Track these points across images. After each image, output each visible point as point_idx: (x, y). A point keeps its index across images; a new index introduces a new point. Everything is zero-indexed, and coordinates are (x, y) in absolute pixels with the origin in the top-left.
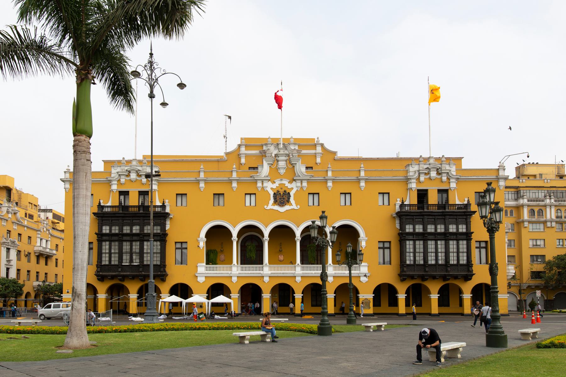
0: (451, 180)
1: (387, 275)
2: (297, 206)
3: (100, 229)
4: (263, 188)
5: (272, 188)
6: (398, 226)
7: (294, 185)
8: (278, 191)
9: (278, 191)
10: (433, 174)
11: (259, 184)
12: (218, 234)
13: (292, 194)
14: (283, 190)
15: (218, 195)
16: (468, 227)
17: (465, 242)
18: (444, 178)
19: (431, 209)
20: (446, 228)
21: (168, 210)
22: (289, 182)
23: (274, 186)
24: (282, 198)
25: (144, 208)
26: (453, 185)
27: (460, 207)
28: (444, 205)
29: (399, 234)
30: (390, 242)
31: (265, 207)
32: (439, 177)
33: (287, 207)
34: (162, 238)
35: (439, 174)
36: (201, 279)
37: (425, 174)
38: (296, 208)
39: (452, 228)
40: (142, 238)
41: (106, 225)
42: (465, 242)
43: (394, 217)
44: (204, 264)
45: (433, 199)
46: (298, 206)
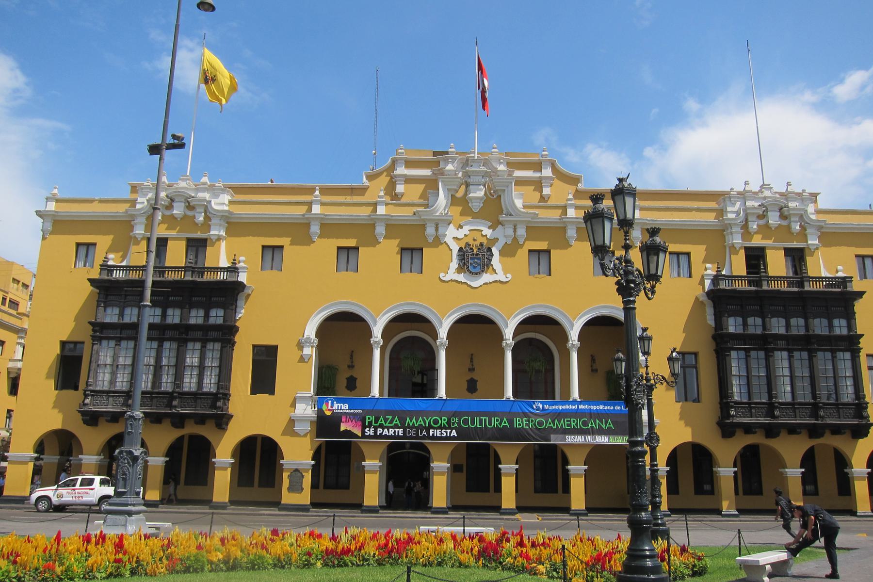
0: (808, 231)
2: (505, 274)
5: (456, 239)
6: (710, 321)
7: (499, 232)
8: (468, 245)
9: (468, 245)
11: (430, 230)
14: (478, 243)
16: (851, 326)
17: (848, 355)
19: (775, 286)
22: (489, 228)
23: (460, 234)
24: (474, 259)
29: (714, 337)
30: (696, 354)
31: (442, 275)
33: (486, 277)
35: (783, 217)
38: (504, 280)
43: (702, 302)
46: (509, 276)
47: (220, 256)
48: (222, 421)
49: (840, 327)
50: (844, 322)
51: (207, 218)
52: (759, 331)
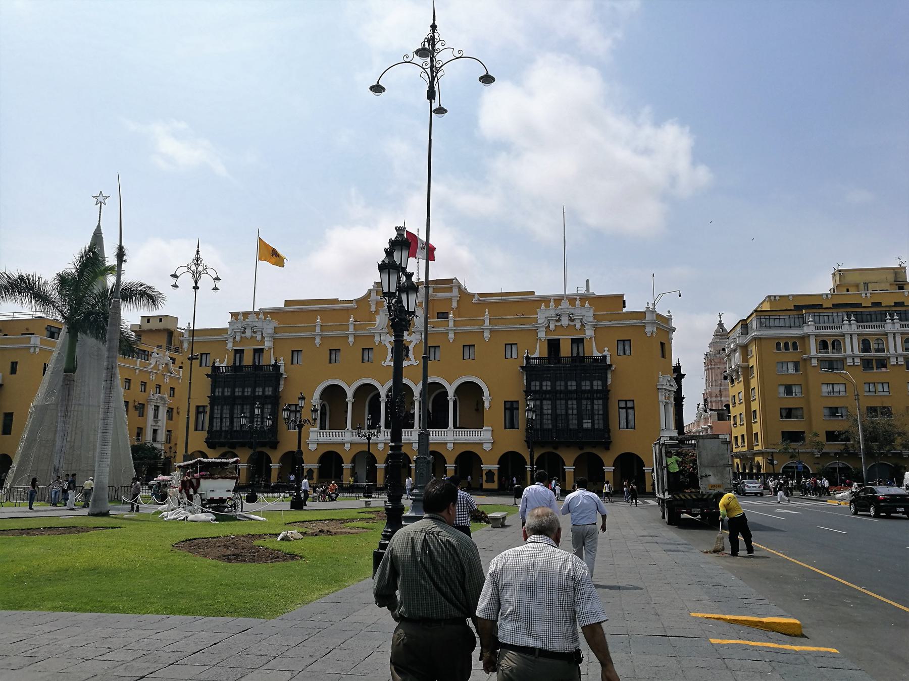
1: (515, 441)
3: (213, 391)
4: (380, 342)
10: (565, 321)
11: (377, 338)
12: (333, 394)
13: (411, 347)
15: (334, 352)
18: (578, 326)
20: (579, 385)
21: (282, 370)
25: (257, 367)
26: (589, 333)
27: (595, 360)
28: (578, 359)
32: (572, 323)
34: (275, 400)
36: (312, 447)
37: (557, 321)
39: (586, 385)
40: (251, 401)
41: (259, 387)
42: (601, 402)
44: (317, 429)
45: (566, 350)
47: (269, 359)
48: (274, 445)
49: (597, 385)
50: (600, 383)
51: (263, 338)
52: (588, 388)
